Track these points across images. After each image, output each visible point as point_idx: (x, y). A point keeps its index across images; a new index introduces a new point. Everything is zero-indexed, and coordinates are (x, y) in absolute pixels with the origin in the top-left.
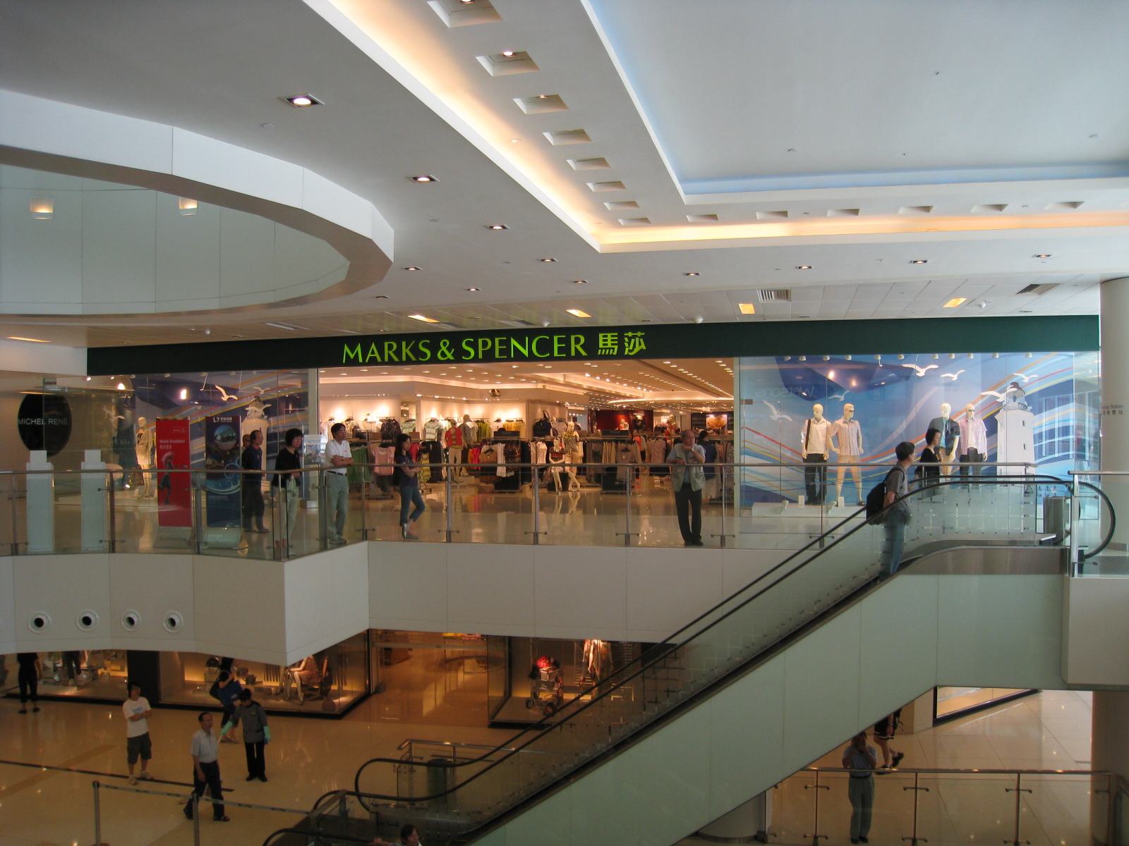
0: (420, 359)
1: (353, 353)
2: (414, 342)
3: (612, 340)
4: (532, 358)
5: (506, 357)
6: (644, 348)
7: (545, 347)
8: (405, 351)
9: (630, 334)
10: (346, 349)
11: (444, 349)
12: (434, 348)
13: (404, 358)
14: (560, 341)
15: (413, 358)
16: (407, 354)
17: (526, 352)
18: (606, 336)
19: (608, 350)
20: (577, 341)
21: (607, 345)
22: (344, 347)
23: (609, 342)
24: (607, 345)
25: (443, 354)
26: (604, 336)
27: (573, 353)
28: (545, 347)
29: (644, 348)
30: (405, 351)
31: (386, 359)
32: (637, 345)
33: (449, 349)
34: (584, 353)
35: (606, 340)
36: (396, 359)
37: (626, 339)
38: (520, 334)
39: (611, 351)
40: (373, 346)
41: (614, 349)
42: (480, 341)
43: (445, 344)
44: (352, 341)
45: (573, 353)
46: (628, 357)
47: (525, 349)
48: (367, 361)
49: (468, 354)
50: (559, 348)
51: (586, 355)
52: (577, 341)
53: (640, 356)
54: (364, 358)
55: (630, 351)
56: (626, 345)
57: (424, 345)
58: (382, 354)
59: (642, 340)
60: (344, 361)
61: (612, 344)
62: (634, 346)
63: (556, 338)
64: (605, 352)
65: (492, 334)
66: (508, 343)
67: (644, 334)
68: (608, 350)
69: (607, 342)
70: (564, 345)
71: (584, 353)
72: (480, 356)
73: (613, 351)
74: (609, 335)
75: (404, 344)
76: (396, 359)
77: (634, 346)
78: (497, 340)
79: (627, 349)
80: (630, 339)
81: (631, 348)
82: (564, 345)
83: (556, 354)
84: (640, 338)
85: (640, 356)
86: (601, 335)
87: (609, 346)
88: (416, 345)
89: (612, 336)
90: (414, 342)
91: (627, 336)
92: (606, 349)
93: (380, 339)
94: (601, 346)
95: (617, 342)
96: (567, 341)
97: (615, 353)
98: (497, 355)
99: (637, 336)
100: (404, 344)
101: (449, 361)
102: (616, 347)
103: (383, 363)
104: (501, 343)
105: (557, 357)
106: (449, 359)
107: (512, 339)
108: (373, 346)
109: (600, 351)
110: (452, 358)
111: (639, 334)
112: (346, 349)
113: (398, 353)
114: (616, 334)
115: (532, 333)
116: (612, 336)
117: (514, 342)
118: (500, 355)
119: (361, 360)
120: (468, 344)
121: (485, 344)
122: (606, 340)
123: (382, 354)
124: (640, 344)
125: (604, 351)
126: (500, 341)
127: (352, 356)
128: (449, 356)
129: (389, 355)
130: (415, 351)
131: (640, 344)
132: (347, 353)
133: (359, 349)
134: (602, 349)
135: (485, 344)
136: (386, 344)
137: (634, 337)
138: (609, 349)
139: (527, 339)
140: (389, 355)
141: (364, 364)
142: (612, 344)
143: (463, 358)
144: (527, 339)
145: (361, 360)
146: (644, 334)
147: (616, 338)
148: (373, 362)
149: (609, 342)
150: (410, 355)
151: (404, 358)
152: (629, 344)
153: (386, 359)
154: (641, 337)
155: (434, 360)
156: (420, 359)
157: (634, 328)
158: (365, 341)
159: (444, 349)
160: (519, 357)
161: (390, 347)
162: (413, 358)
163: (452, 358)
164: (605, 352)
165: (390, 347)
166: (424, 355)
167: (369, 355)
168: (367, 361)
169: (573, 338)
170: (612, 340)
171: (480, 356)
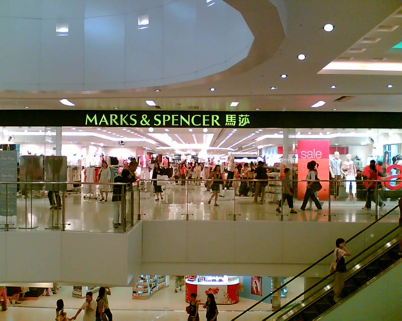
0: (131, 124)
1: (91, 119)
2: (127, 115)
3: (233, 118)
4: (191, 126)
5: (209, 125)
6: (249, 123)
7: (198, 121)
8: (122, 119)
9: (242, 116)
10: (88, 117)
11: (144, 119)
12: (139, 119)
13: (122, 124)
14: (206, 118)
15: (127, 124)
16: (123, 122)
17: (188, 123)
18: (230, 116)
19: (230, 123)
20: (215, 118)
21: (230, 120)
22: (94, 115)
23: (231, 119)
24: (230, 120)
25: (144, 122)
26: (229, 116)
27: (213, 124)
28: (198, 121)
29: (249, 123)
30: (122, 119)
31: (111, 124)
32: (245, 120)
33: (147, 120)
34: (218, 125)
35: (230, 118)
36: (117, 124)
37: (240, 118)
38: (185, 114)
39: (232, 123)
40: (104, 116)
41: (233, 122)
42: (164, 116)
43: (145, 117)
44: (91, 113)
45: (213, 124)
46: (241, 127)
47: (188, 121)
48: (100, 124)
49: (157, 123)
50: (206, 121)
51: (220, 125)
52: (215, 118)
53: (247, 126)
54: (98, 123)
55: (242, 124)
56: (240, 121)
57: (133, 117)
58: (109, 122)
59: (248, 119)
60: (86, 124)
61: (233, 120)
62: (244, 122)
63: (204, 116)
64: (229, 124)
65: (171, 113)
66: (179, 118)
67: (249, 116)
68: (230, 123)
69: (230, 119)
70: (208, 120)
71: (218, 125)
72: (164, 124)
73: (233, 124)
74: (231, 116)
75: (122, 116)
76: (117, 124)
77: (244, 122)
78: (173, 116)
79: (240, 123)
80: (242, 118)
81: (242, 123)
82: (208, 120)
83: (204, 124)
84: (247, 117)
85: (247, 126)
86: (227, 116)
87: (231, 121)
88: (129, 117)
89: (233, 116)
90: (127, 115)
91: (241, 117)
92: (230, 122)
93: (108, 113)
94: (227, 121)
95: (235, 119)
96: (210, 118)
97: (234, 125)
98: (173, 124)
99: (245, 117)
100: (122, 116)
101: (147, 126)
102: (235, 122)
103: (109, 126)
104: (175, 118)
105: (173, 126)
106: (147, 125)
107: (104, 115)
108: (104, 116)
109: (226, 123)
110: (148, 124)
111: (246, 116)
112: (88, 117)
113: (118, 120)
114: (235, 115)
115: (192, 113)
116: (233, 116)
117: (182, 117)
118: (205, 124)
119: (96, 124)
120: (157, 117)
121: (167, 118)
122: (230, 118)
123: (109, 122)
124: (247, 121)
125: (228, 123)
126: (206, 117)
127: (91, 121)
128: (147, 123)
129: (113, 121)
130: (128, 119)
131: (247, 121)
132: (88, 119)
133: (95, 117)
134: (228, 122)
135: (167, 118)
136: (111, 116)
137: (244, 117)
138: (232, 122)
139: (189, 116)
140: (113, 121)
141: (98, 126)
142: (233, 120)
143: (155, 124)
144: (189, 116)
145: (96, 124)
146: (249, 116)
147: (235, 117)
148: (104, 125)
149: (231, 119)
150: (125, 122)
151: (122, 124)
152: (241, 120)
153: (111, 124)
154: (248, 117)
155: (138, 125)
156: (131, 124)
157: (244, 113)
158: (99, 113)
159: (144, 119)
160: (185, 125)
161: (114, 117)
162: (127, 124)
163: (148, 124)
164: (229, 124)
165: (114, 117)
166: (133, 122)
167: (101, 121)
168: (100, 124)
169: (213, 116)
170: (233, 118)
171: (164, 124)
